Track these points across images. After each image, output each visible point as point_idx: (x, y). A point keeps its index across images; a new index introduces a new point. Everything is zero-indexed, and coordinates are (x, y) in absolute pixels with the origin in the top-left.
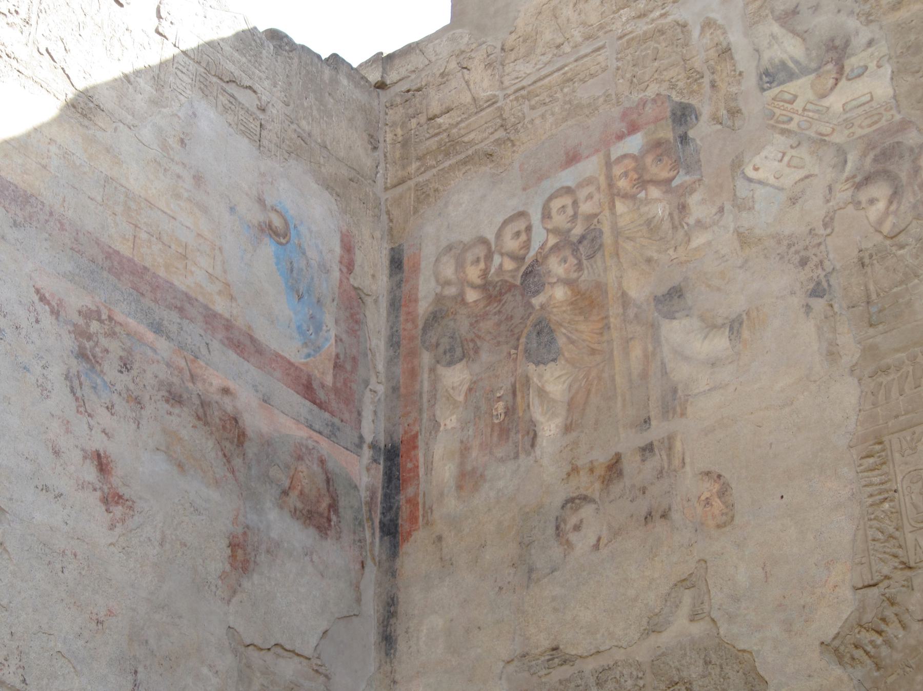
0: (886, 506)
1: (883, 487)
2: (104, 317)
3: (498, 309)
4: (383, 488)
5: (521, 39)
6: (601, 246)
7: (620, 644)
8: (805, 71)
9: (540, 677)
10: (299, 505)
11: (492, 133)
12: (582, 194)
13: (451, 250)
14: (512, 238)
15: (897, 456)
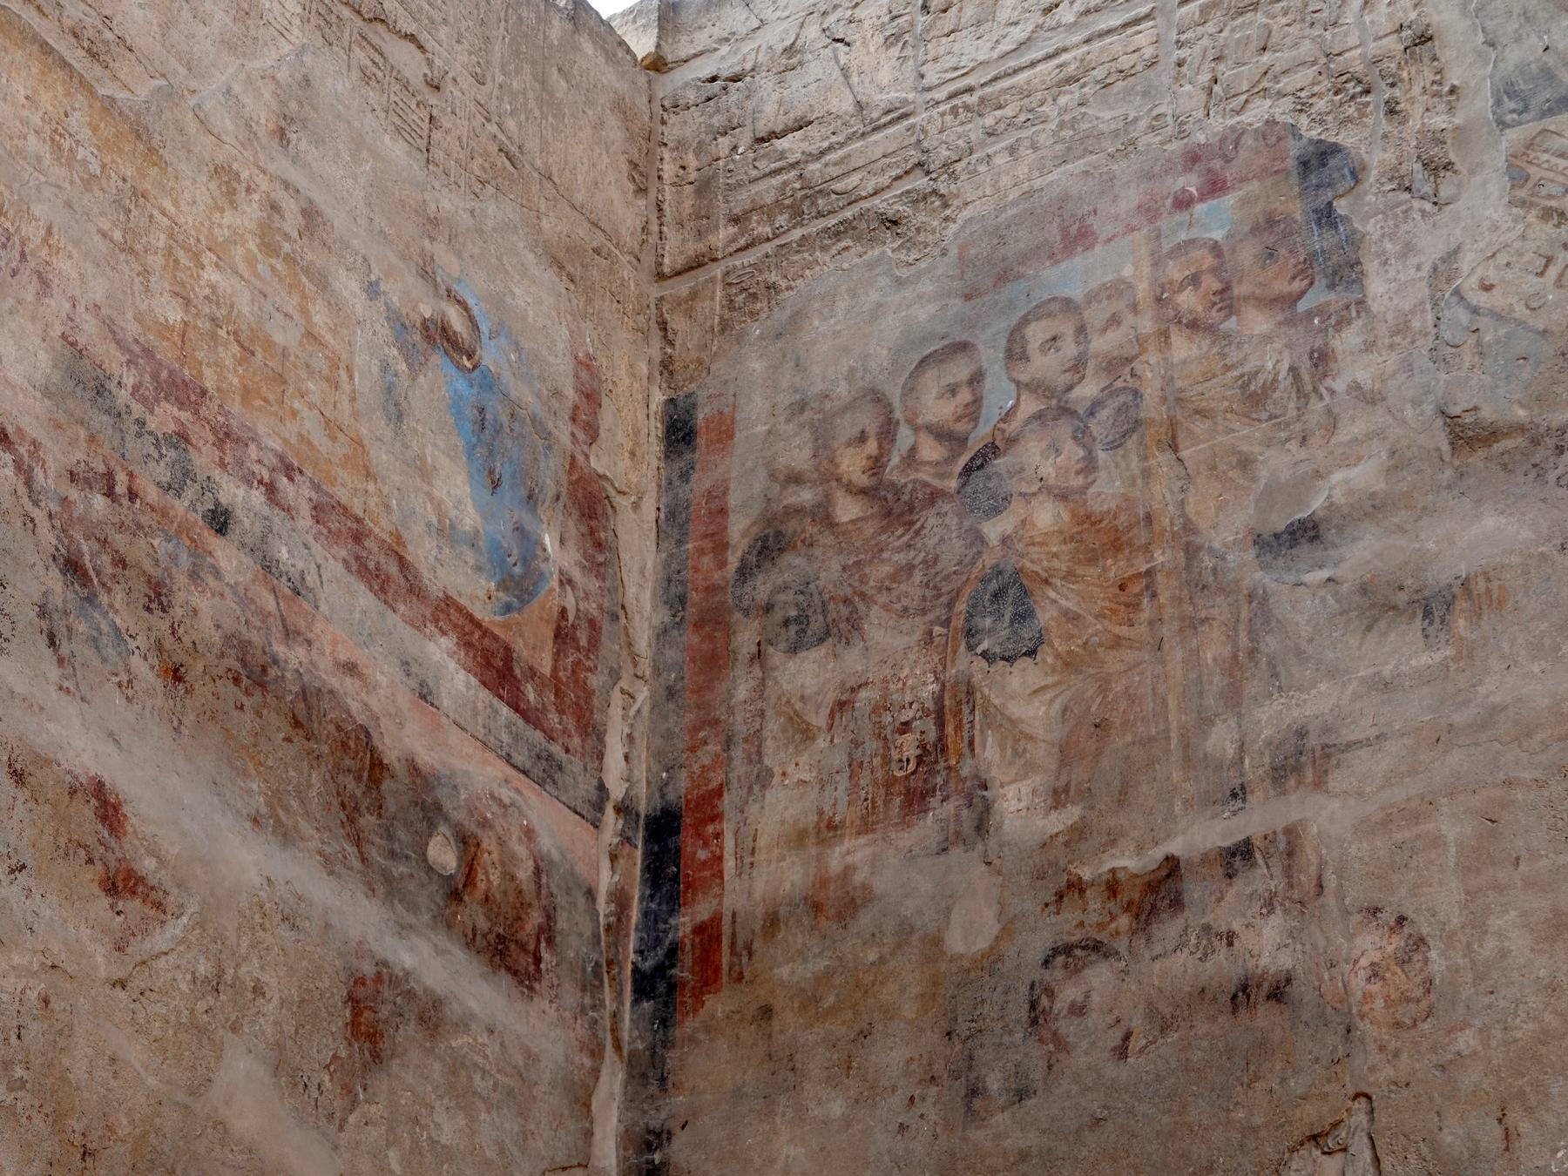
2: (120, 489)
3: (905, 539)
6: (1138, 423)
10: (483, 924)
11: (898, 178)
12: (1095, 315)
13: (802, 410)
14: (940, 396)
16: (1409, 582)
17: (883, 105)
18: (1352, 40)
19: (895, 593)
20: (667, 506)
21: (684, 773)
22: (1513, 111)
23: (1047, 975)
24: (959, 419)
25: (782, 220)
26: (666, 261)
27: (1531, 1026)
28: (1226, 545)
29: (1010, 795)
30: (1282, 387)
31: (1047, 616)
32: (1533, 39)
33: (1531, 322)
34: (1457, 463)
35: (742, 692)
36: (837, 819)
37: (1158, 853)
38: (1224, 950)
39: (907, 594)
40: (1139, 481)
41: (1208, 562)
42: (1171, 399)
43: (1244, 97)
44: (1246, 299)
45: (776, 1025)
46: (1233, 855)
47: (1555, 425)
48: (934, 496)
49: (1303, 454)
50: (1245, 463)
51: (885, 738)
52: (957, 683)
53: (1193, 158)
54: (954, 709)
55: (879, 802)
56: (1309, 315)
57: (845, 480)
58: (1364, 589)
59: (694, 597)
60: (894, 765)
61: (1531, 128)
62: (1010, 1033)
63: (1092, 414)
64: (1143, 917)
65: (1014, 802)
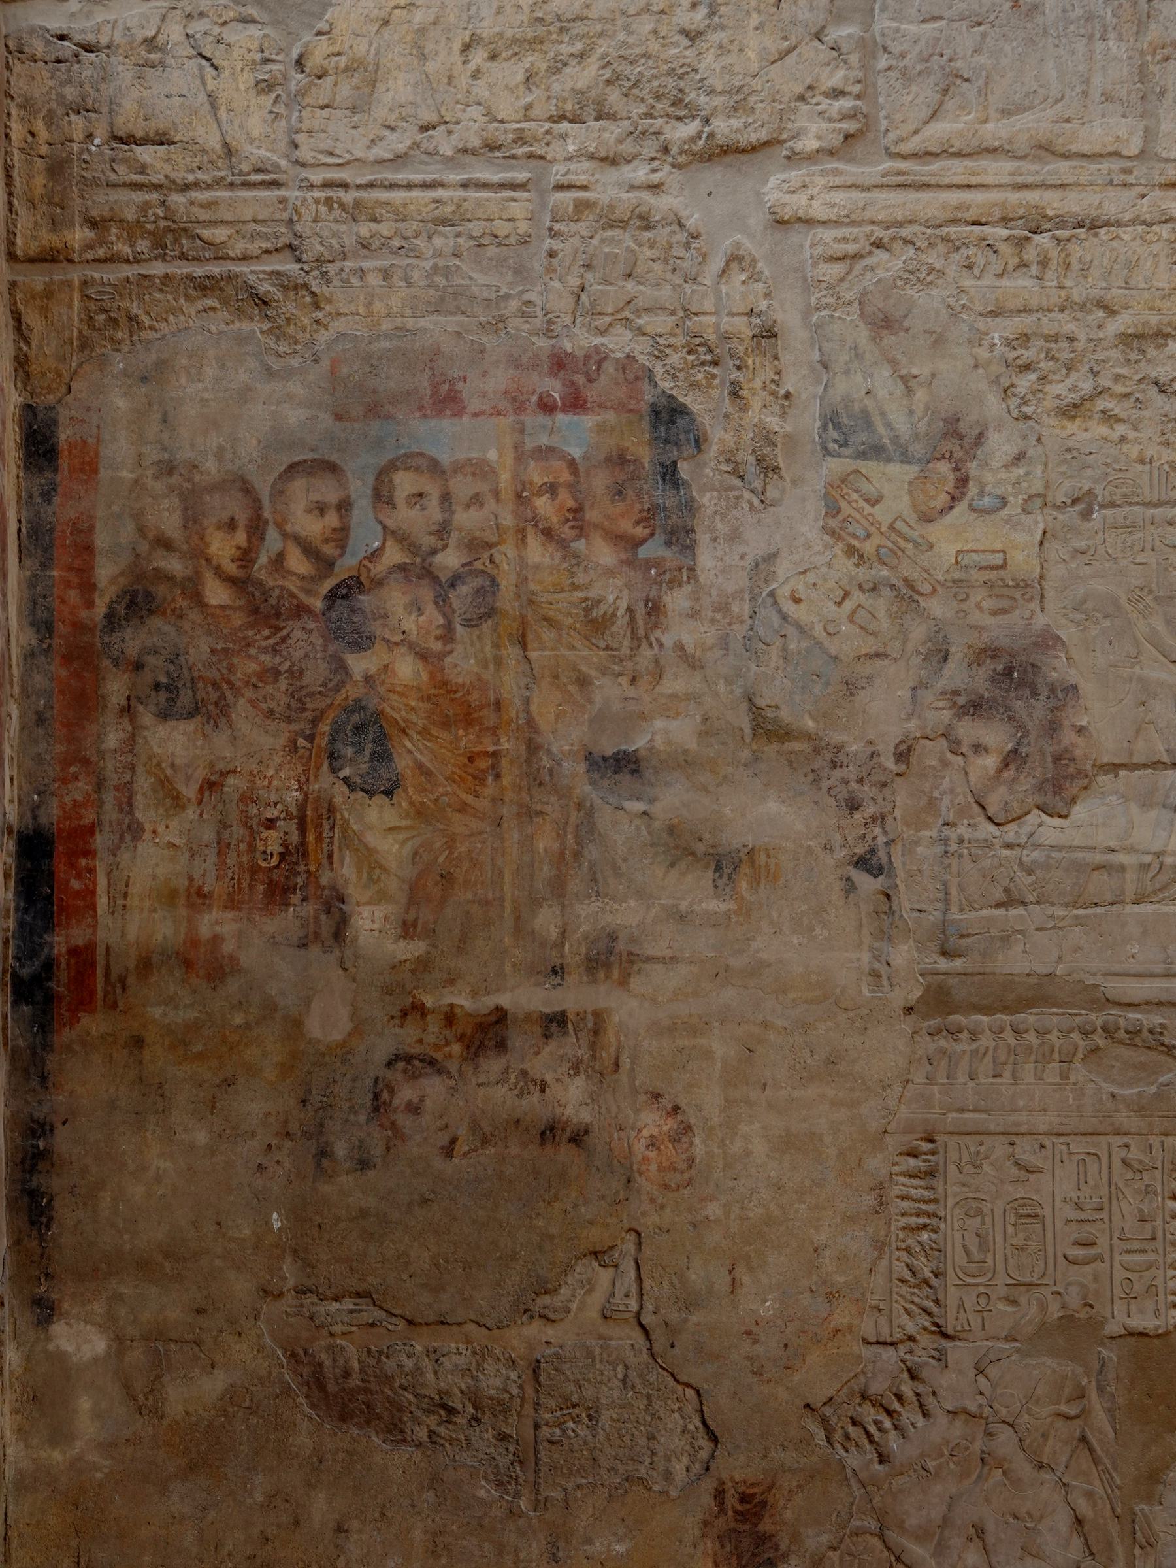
0: (925, 1236)
1: (924, 1207)
3: (272, 641)
4: (17, 909)
5: (343, 61)
6: (491, 612)
7: (483, 1321)
8: (906, 458)
9: (332, 1335)
11: (267, 252)
12: (463, 488)
14: (309, 511)
15: (952, 1169)
16: (707, 836)
17: (253, 160)
18: (709, 305)
19: (261, 693)
20: (29, 522)
21: (55, 802)
22: (835, 441)
23: (389, 1074)
24: (327, 541)
25: (143, 245)
26: (19, 241)
27: (761, 1211)
28: (562, 751)
29: (365, 915)
30: (619, 622)
31: (403, 763)
32: (859, 378)
33: (826, 644)
34: (755, 747)
35: (113, 740)
36: (206, 889)
37: (489, 1002)
38: (537, 1094)
39: (273, 698)
40: (491, 666)
41: (546, 762)
42: (524, 598)
43: (608, 319)
44: (596, 526)
45: (147, 1055)
46: (551, 1021)
47: (833, 742)
48: (301, 610)
49: (631, 692)
50: (583, 682)
51: (251, 828)
52: (318, 799)
53: (559, 363)
54: (313, 817)
55: (245, 885)
56: (648, 564)
57: (214, 562)
58: (671, 830)
59: (61, 628)
60: (258, 855)
61: (847, 465)
62: (356, 1113)
63: (453, 585)
64: (473, 1050)
65: (368, 922)
